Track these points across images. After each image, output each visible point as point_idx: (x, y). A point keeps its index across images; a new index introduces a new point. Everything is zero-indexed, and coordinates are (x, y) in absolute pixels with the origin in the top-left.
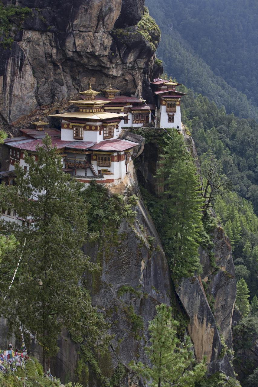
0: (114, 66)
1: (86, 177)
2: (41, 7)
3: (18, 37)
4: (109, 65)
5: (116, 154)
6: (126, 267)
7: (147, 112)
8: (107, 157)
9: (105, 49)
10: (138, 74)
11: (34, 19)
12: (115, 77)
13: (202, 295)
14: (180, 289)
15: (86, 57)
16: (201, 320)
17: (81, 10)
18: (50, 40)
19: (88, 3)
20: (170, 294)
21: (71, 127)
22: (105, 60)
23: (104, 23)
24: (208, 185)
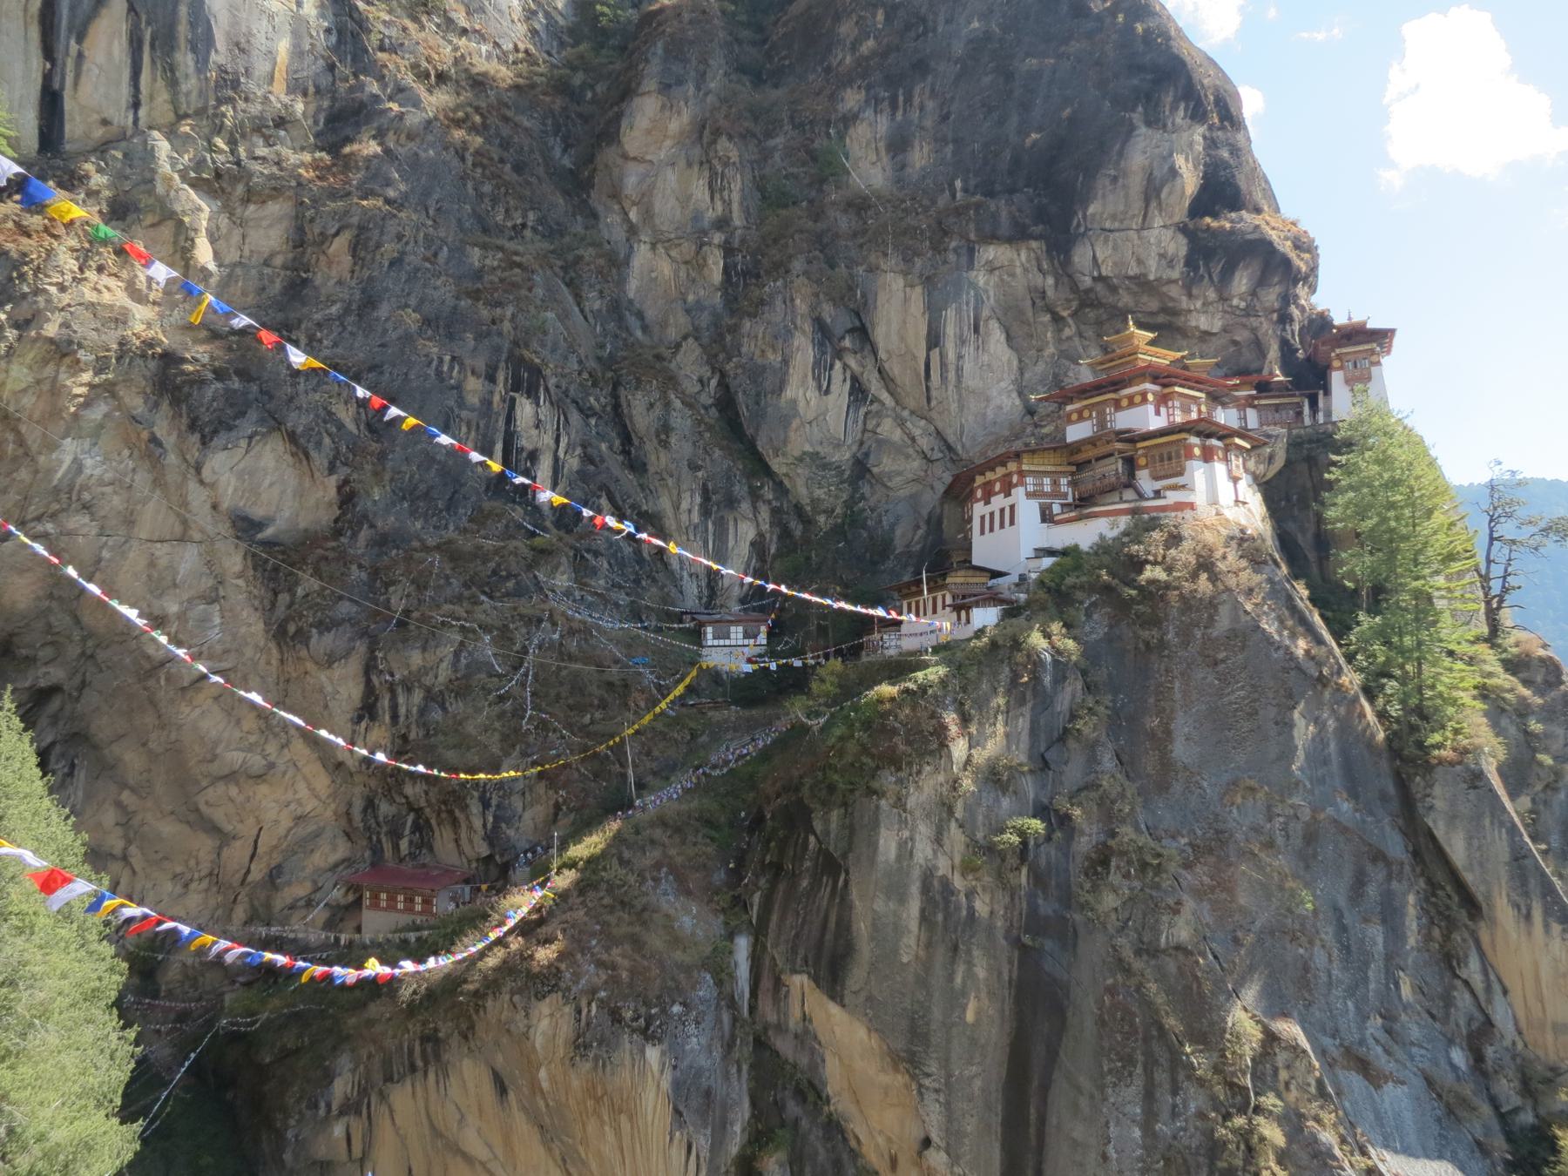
0: (1199, 304)
1: (1122, 501)
2: (1012, 191)
3: (964, 260)
4: (1184, 303)
5: (1194, 440)
6: (1246, 726)
7: (1296, 400)
8: (1173, 449)
9: (1171, 264)
10: (1265, 326)
11: (995, 217)
12: (1206, 335)
13: (1514, 825)
14: (1431, 808)
15: (1128, 289)
16: (1524, 911)
17: (1102, 182)
18: (1038, 259)
19: (1117, 163)
20: (1401, 822)
21: (1086, 414)
22: (1174, 291)
23: (1160, 204)
24: (1491, 544)
